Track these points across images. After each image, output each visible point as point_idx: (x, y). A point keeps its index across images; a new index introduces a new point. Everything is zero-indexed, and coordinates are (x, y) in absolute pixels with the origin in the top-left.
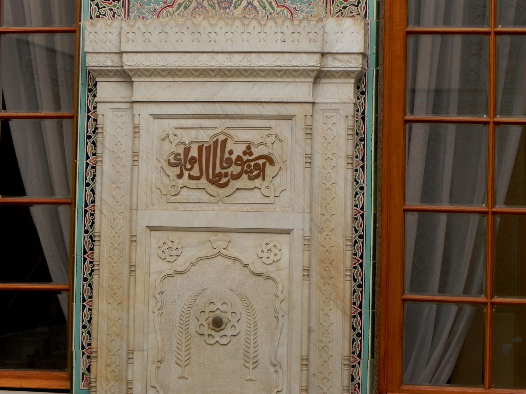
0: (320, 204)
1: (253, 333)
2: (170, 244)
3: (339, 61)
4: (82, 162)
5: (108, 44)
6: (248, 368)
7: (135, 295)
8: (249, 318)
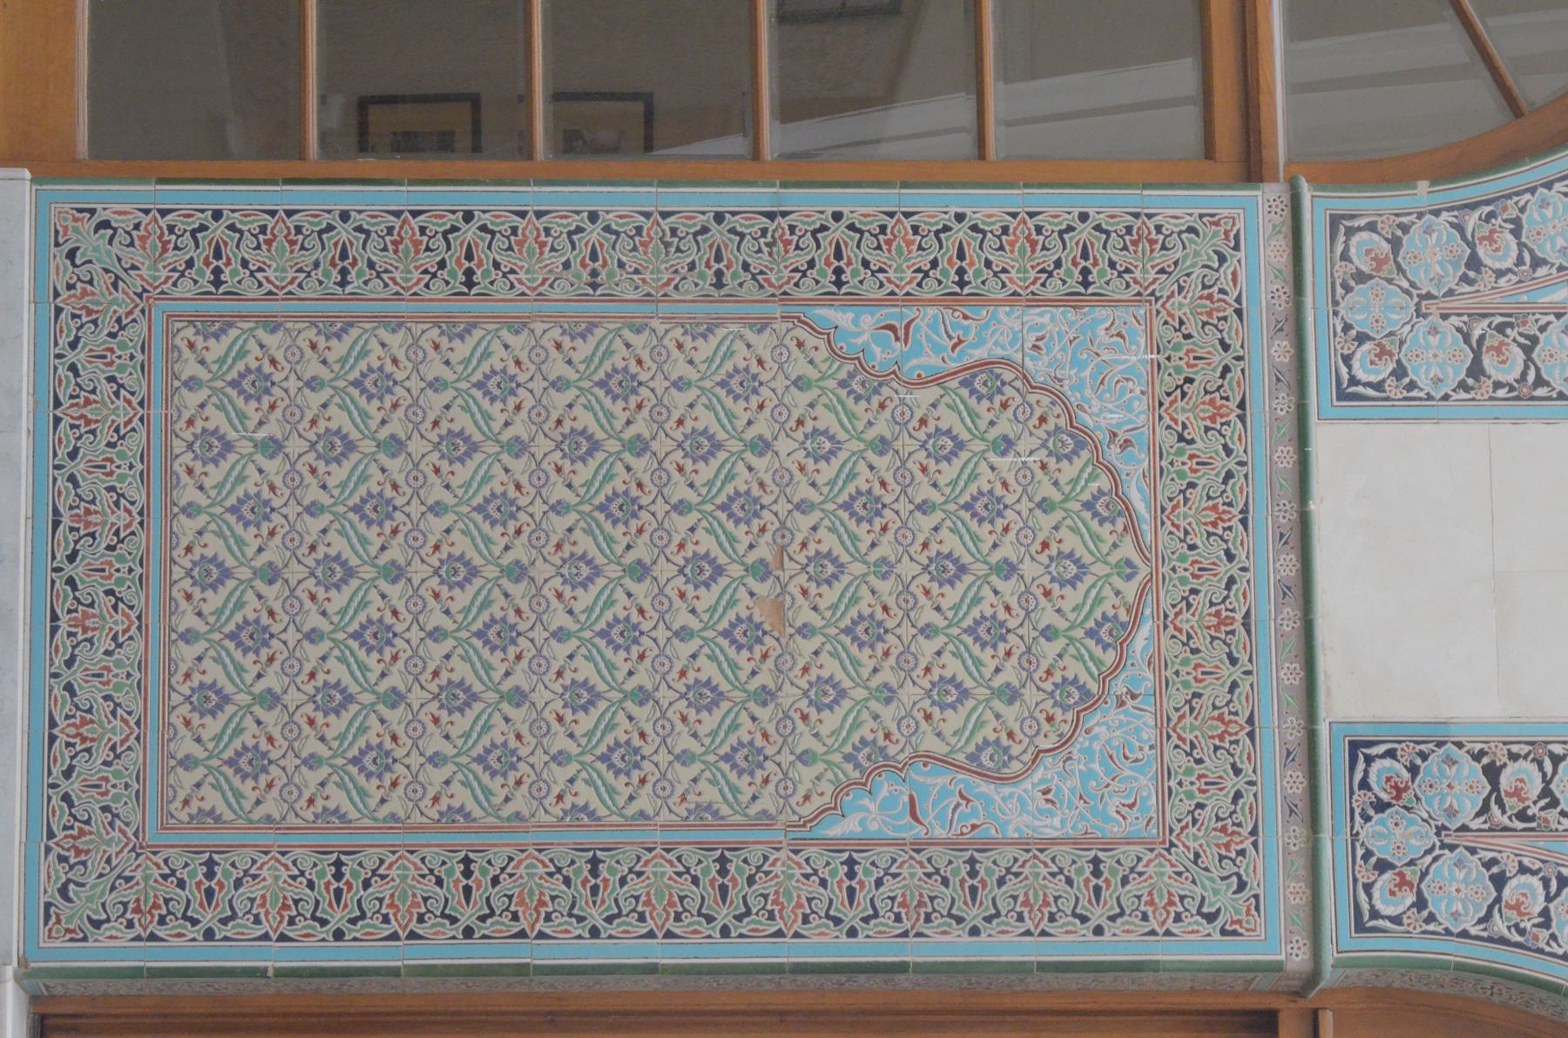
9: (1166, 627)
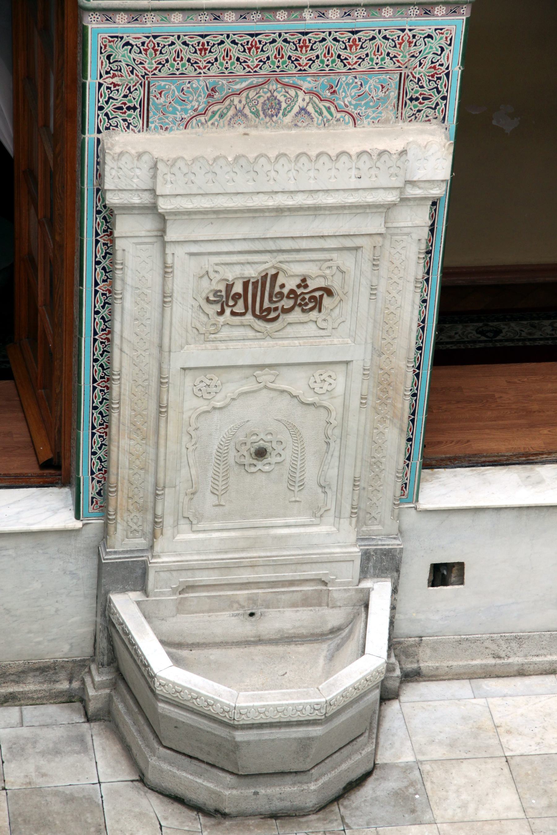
0: (381, 329)
1: (300, 458)
2: (208, 382)
3: (419, 188)
4: (90, 290)
5: (135, 180)
6: (293, 491)
7: (166, 435)
8: (296, 445)
9: (305, 70)
